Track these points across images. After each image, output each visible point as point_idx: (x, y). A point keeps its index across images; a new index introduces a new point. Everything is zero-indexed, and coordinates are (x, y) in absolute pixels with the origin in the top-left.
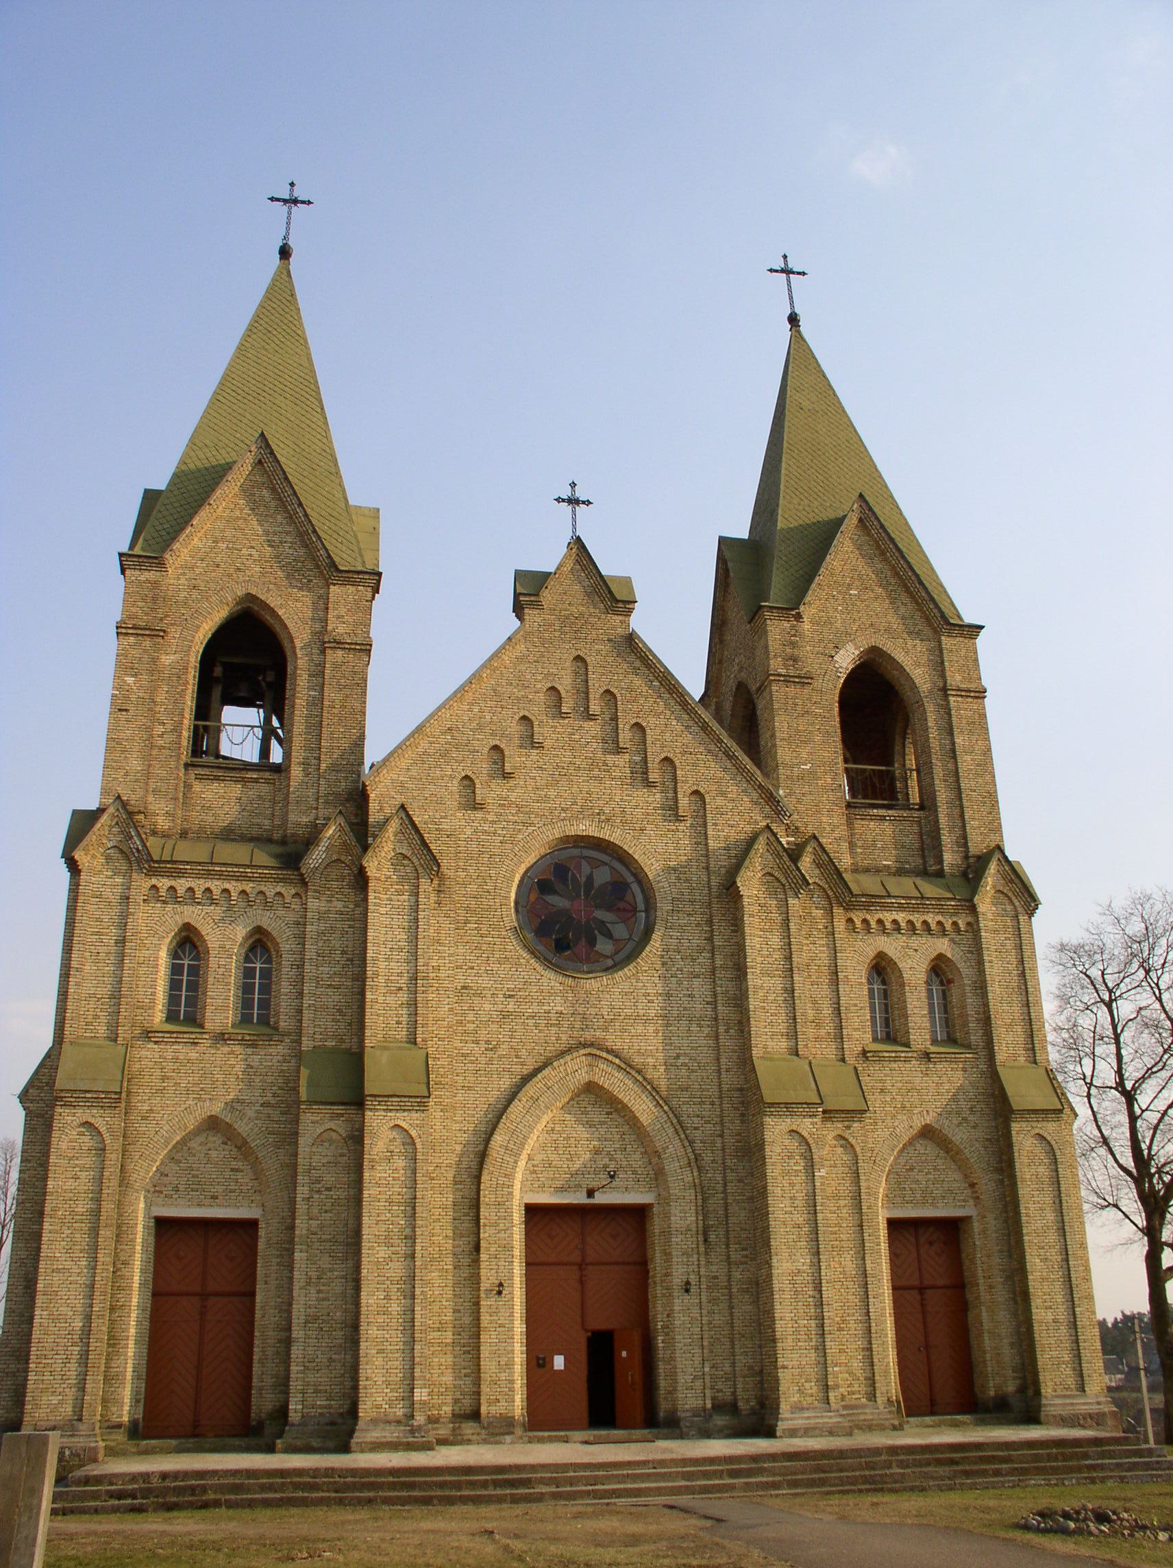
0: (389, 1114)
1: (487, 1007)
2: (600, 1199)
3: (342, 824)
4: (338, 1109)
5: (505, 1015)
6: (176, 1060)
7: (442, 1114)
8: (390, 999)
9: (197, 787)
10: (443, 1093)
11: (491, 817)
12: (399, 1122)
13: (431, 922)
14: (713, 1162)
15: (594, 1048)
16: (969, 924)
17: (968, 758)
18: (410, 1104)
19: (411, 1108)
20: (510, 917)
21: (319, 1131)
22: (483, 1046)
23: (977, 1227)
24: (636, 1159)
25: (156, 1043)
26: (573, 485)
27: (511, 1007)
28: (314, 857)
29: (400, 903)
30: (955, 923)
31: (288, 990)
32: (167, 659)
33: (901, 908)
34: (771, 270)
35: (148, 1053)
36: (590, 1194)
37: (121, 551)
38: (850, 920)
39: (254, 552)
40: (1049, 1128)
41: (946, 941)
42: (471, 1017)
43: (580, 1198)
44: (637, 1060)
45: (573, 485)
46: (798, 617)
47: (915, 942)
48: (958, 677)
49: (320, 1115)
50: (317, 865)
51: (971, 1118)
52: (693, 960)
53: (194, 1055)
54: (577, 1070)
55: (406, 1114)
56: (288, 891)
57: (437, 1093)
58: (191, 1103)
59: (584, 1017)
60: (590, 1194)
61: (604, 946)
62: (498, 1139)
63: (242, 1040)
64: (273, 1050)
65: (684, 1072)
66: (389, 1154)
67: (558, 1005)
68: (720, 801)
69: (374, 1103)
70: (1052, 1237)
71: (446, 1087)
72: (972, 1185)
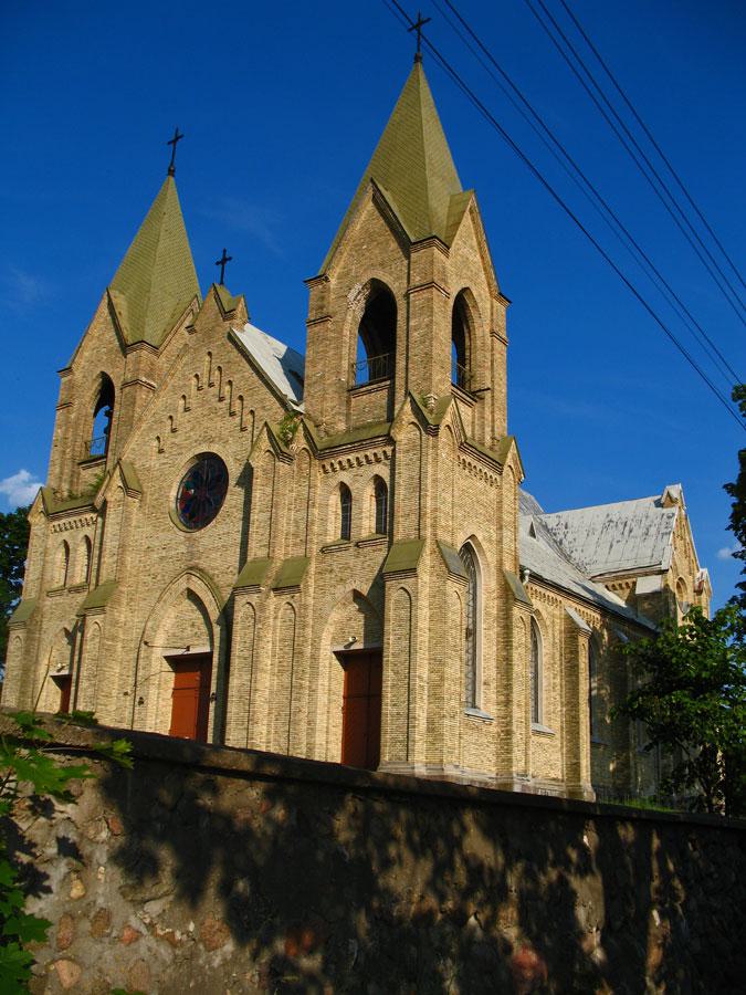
5: (162, 558)
8: (111, 560)
9: (83, 473)
13: (136, 516)
15: (193, 570)
17: (416, 334)
32: (73, 416)
33: (350, 451)
35: (48, 602)
38: (324, 467)
40: (408, 583)
41: (380, 465)
44: (211, 572)
46: (327, 280)
48: (418, 278)
54: (182, 584)
59: (192, 553)
60: (188, 649)
62: (150, 624)
67: (183, 549)
70: (404, 657)
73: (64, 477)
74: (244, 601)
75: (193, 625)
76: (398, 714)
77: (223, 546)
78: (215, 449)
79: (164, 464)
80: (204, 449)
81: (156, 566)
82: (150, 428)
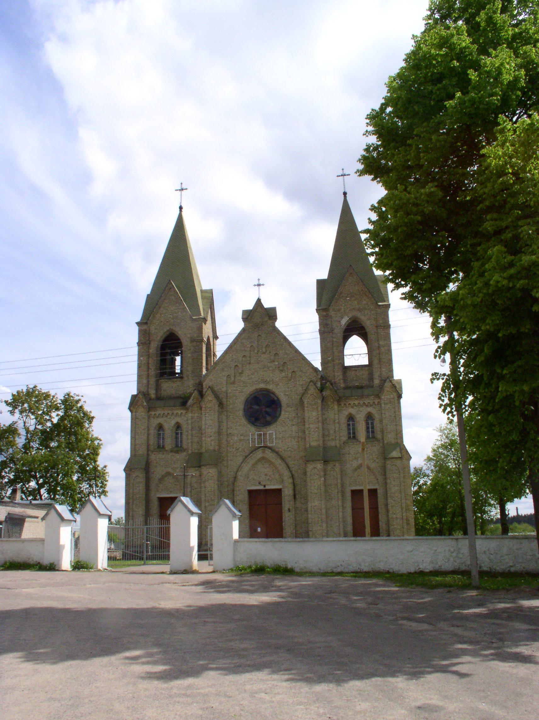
1: (236, 438)
2: (267, 487)
4: (197, 468)
5: (241, 440)
6: (159, 458)
11: (236, 386)
14: (298, 476)
16: (378, 402)
20: (241, 413)
22: (235, 449)
23: (378, 491)
24: (277, 476)
26: (259, 280)
27: (242, 438)
30: (374, 402)
34: (338, 176)
36: (265, 486)
37: (137, 322)
39: (171, 316)
42: (232, 441)
43: (261, 488)
44: (277, 450)
45: (259, 280)
47: (361, 409)
51: (377, 460)
52: (293, 420)
53: (163, 457)
56: (184, 412)
60: (265, 486)
61: (268, 418)
62: (239, 473)
65: (289, 452)
68: (300, 373)
72: (377, 479)
73: (150, 386)
74: (312, 467)
75: (266, 475)
76: (397, 518)
77: (283, 437)
78: (270, 387)
79: (235, 390)
80: (262, 386)
81: (238, 444)
82: (223, 370)
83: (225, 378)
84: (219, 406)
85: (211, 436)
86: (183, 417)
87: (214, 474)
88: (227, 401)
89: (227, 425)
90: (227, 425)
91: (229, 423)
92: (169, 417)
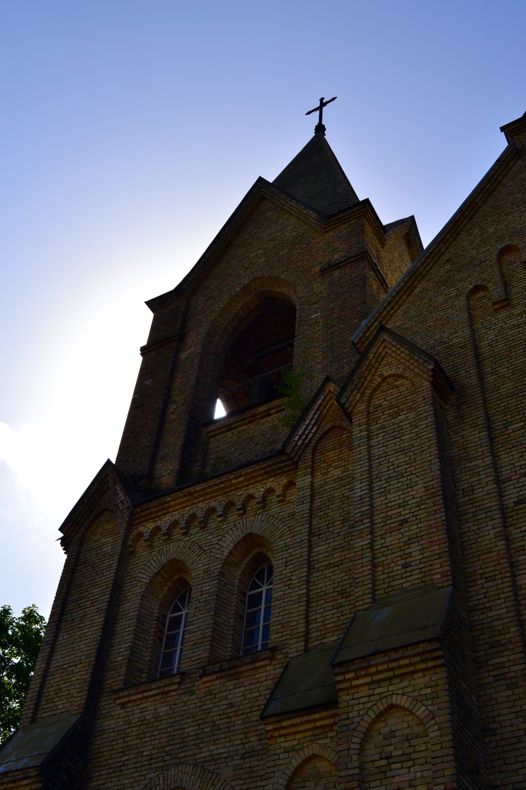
0: (377, 691)
3: (332, 390)
7: (509, 693)
10: (505, 659)
12: (395, 700)
18: (407, 661)
19: (411, 669)
21: (295, 763)
25: (123, 706)
28: (300, 433)
29: (396, 426)
31: (282, 593)
49: (298, 736)
50: (306, 442)
53: (163, 710)
55: (405, 684)
57: (494, 661)
58: (152, 775)
63: (221, 671)
64: (261, 675)
66: (384, 762)
69: (348, 676)
71: (510, 646)
83: (462, 302)
84: (434, 384)
85: (405, 521)
86: (275, 509)
87: (421, 711)
88: (481, 375)
89: (496, 466)
90: (496, 466)
91: (504, 459)
92: (212, 525)
